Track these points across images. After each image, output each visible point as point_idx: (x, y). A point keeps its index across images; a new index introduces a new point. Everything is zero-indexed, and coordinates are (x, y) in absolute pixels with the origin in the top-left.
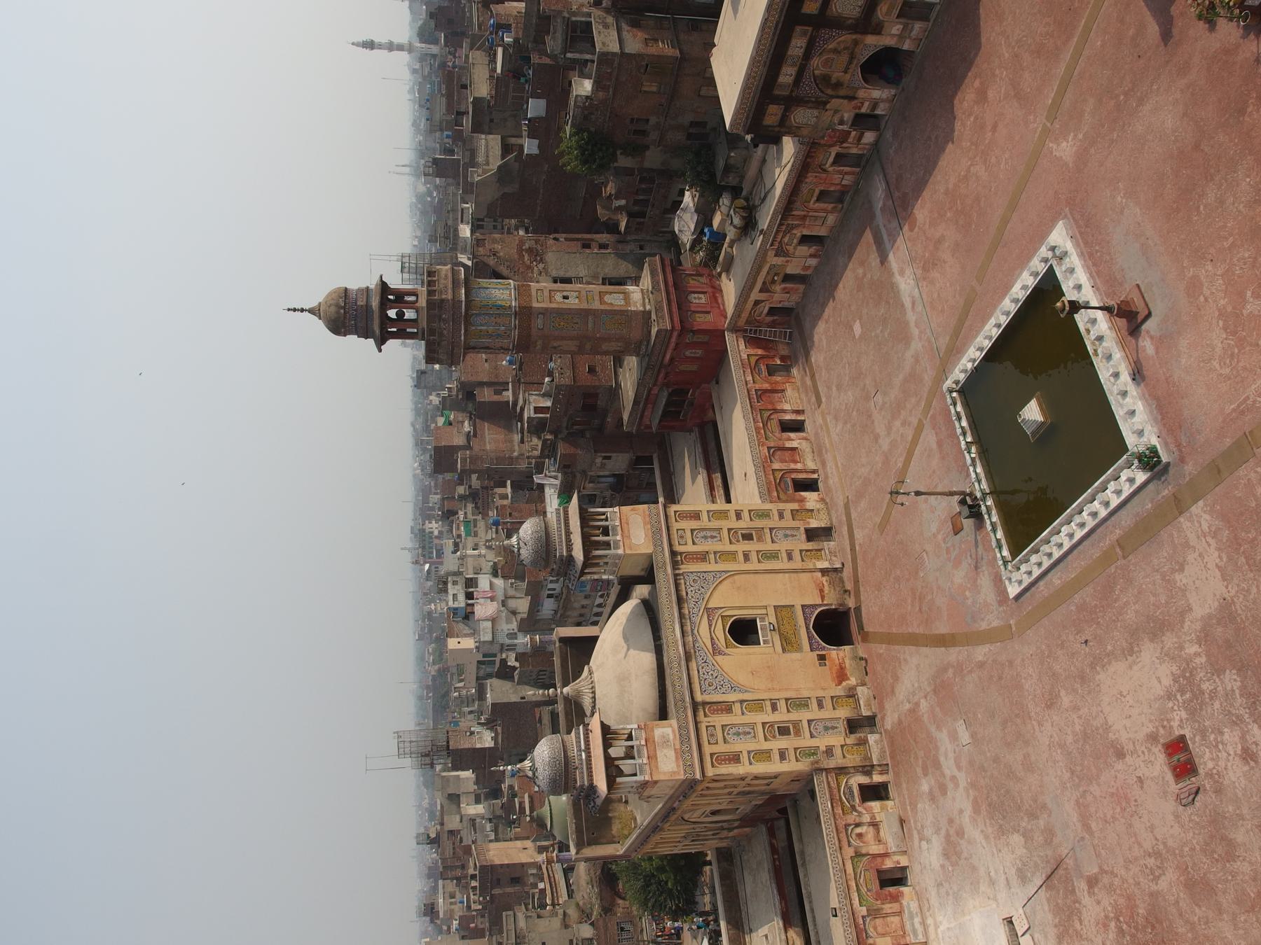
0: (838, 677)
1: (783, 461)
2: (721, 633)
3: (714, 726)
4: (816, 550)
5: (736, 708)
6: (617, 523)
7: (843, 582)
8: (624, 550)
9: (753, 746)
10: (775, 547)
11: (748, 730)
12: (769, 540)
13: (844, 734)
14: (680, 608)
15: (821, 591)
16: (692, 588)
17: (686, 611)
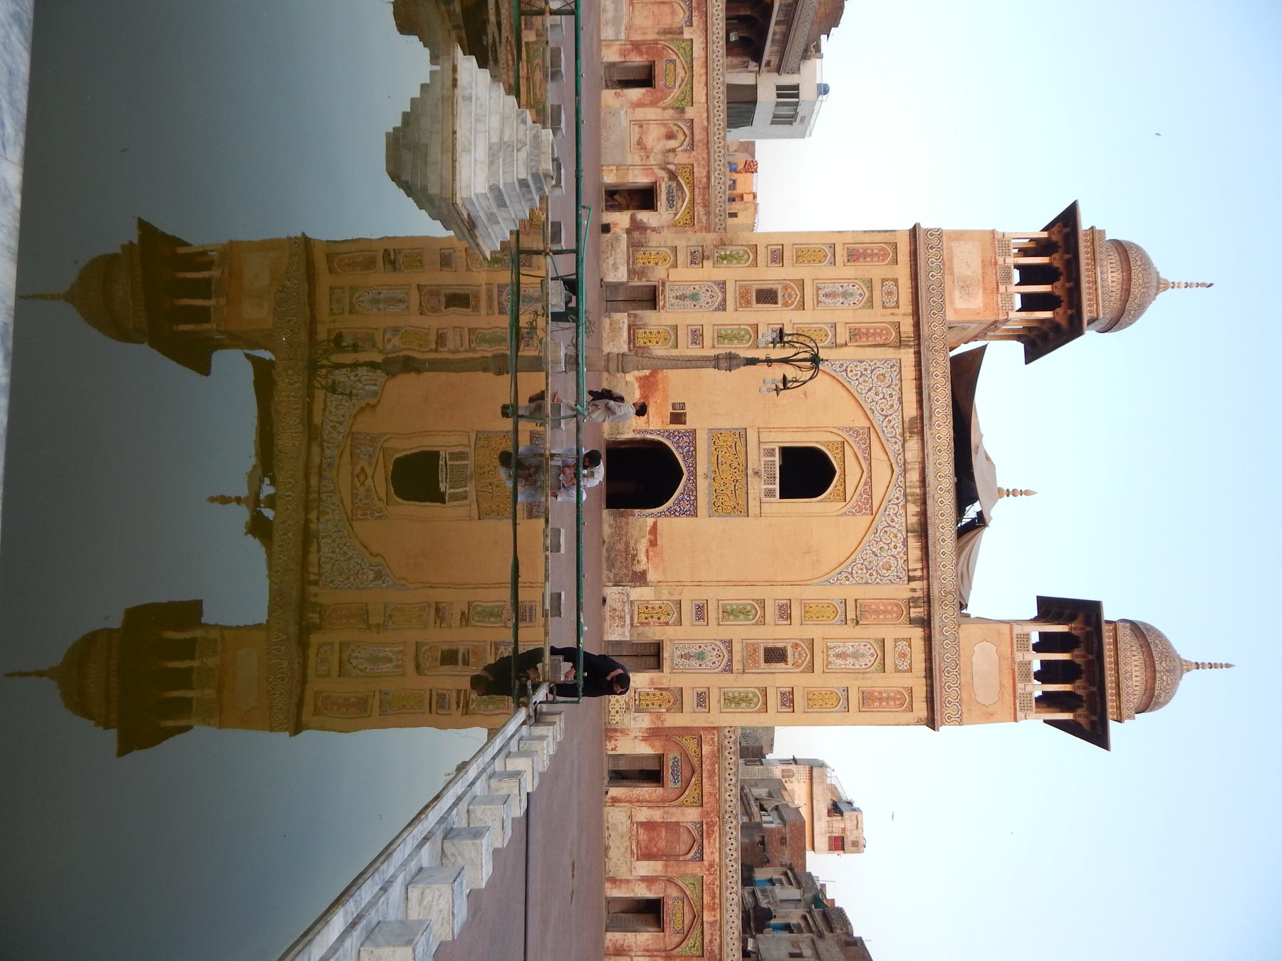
0: (655, 383)
1: (674, 827)
2: (849, 472)
3: (884, 307)
4: (648, 624)
5: (843, 336)
6: (1020, 686)
7: (608, 558)
8: (1012, 634)
9: (826, 272)
10: (726, 632)
11: (827, 300)
12: (737, 647)
13: (667, 284)
14: (923, 514)
15: (653, 543)
16: (894, 552)
17: (913, 509)
